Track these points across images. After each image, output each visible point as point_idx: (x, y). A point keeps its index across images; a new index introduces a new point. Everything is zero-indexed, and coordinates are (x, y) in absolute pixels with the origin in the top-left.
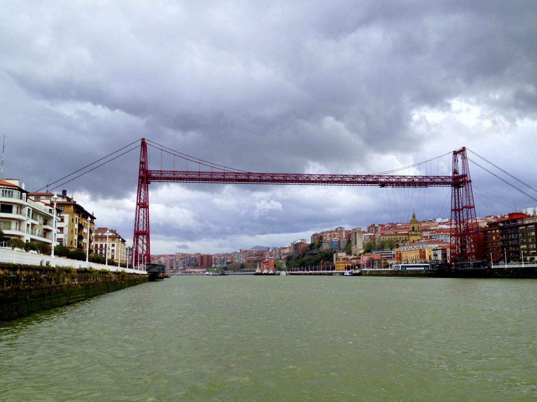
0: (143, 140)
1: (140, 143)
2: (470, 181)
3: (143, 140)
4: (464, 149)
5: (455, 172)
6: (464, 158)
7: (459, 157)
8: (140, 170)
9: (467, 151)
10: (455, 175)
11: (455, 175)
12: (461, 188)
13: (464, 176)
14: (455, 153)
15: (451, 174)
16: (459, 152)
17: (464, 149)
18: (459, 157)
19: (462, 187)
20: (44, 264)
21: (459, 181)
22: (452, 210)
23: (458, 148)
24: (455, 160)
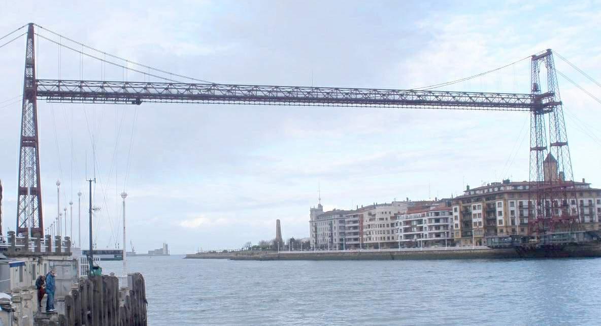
0: (31, 26)
1: (26, 29)
2: (560, 103)
3: (31, 26)
4: (549, 52)
5: (536, 88)
6: (549, 66)
7: (542, 64)
8: (26, 78)
9: (554, 57)
10: (536, 93)
11: (536, 93)
12: (546, 115)
13: (550, 94)
14: (535, 58)
15: (530, 93)
16: (542, 57)
17: (549, 52)
18: (542, 64)
19: (548, 111)
20: (375, 204)
21: (540, 104)
22: (531, 149)
23: (540, 50)
24: (535, 70)
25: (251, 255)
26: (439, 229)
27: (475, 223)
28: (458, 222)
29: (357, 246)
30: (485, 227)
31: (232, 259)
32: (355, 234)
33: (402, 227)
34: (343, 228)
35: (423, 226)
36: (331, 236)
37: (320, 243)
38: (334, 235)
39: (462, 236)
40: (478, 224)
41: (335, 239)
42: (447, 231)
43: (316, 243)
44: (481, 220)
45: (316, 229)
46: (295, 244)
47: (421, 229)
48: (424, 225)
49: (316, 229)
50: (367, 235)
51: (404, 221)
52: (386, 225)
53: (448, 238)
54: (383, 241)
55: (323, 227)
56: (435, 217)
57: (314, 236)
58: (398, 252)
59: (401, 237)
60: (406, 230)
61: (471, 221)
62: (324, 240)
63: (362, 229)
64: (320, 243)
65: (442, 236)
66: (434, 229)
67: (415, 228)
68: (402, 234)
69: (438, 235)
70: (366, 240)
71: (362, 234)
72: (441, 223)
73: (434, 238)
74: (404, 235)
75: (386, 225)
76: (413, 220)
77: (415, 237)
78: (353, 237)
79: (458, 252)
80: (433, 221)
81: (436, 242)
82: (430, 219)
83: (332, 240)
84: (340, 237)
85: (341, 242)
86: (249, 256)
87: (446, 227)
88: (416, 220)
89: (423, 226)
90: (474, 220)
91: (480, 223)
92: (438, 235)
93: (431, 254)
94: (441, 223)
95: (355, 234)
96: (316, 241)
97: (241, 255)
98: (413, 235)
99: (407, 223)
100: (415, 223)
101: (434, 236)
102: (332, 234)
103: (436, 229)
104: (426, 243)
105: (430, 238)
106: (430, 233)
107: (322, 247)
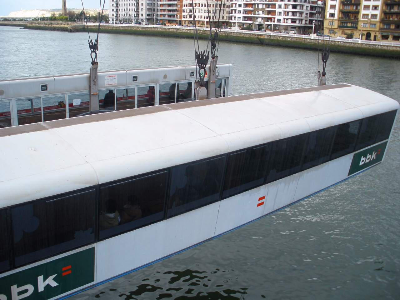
25: (49, 25)
26: (296, 15)
27: (365, 16)
28: (336, 12)
29: (170, 22)
30: (382, 21)
31: (26, 27)
32: (169, 11)
33: (242, 9)
34: (150, 5)
35: (275, 11)
36: (137, 11)
37: (120, 17)
38: (140, 10)
39: (339, 27)
40: (370, 17)
41: (142, 15)
42: (302, 18)
43: (117, 17)
44: (377, 12)
45: (117, 4)
46: (82, 16)
47: (273, 13)
48: (277, 10)
49: (117, 4)
50: (188, 13)
51: (244, 4)
52: (212, 5)
53: (302, 25)
54: (208, 20)
55: (123, 2)
56: (295, 3)
57: (115, 10)
58: (270, 36)
59: (239, 18)
60: (245, 12)
61: (358, 13)
62: (127, 14)
63: (181, 7)
64: (120, 17)
65: (297, 22)
66: (290, 14)
67: (261, 12)
68: (241, 15)
69: (294, 21)
70: (186, 17)
71: (180, 11)
72: (298, 9)
73: (289, 23)
74: (244, 16)
75: (212, 5)
76: (258, 4)
77: (260, 20)
78: (166, 13)
79: (385, 48)
80: (291, 7)
81: (292, 28)
82: (286, 4)
83: (138, 15)
84: (148, 13)
85: (148, 17)
86: (47, 26)
87: (301, 13)
88: (263, 4)
89: (275, 11)
90: (363, 12)
91: (374, 16)
92: (294, 21)
93: (316, 43)
94: (298, 9)
95: (169, 11)
96: (117, 14)
97: (37, 25)
98: (257, 18)
99: (247, 5)
100: (261, 7)
101: (290, 21)
102: (138, 9)
103: (293, 15)
104: (260, 27)
105: (284, 22)
106: (284, 19)
107: (126, 21)
